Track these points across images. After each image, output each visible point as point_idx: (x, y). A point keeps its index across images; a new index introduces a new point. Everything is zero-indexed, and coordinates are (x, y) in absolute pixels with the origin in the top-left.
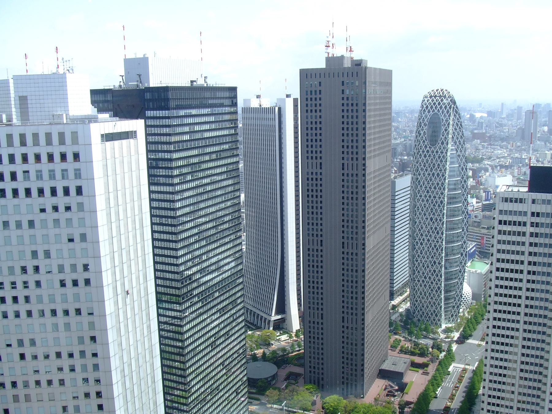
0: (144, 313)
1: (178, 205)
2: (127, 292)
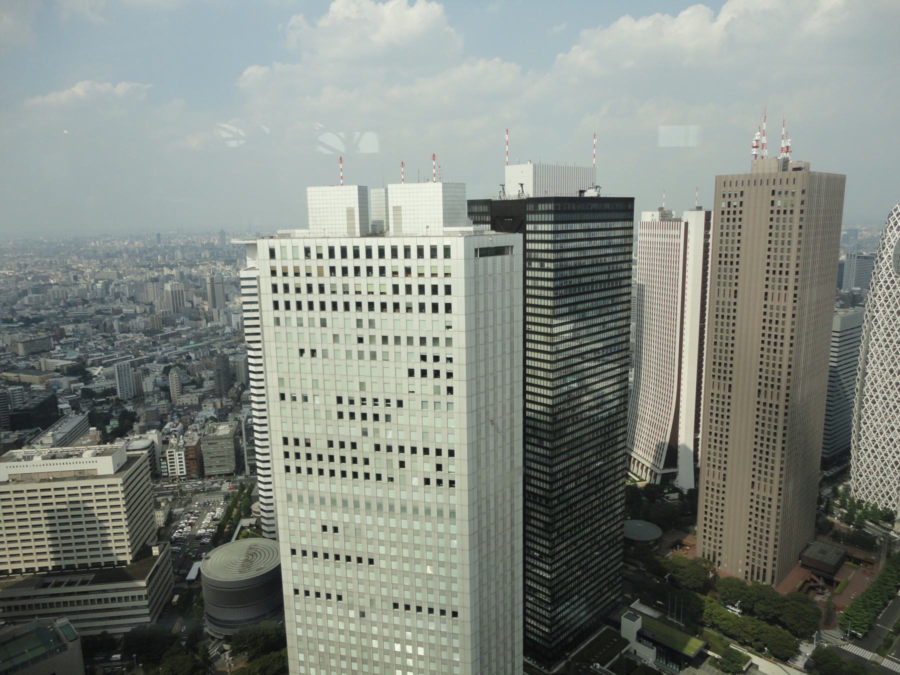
1: (556, 330)
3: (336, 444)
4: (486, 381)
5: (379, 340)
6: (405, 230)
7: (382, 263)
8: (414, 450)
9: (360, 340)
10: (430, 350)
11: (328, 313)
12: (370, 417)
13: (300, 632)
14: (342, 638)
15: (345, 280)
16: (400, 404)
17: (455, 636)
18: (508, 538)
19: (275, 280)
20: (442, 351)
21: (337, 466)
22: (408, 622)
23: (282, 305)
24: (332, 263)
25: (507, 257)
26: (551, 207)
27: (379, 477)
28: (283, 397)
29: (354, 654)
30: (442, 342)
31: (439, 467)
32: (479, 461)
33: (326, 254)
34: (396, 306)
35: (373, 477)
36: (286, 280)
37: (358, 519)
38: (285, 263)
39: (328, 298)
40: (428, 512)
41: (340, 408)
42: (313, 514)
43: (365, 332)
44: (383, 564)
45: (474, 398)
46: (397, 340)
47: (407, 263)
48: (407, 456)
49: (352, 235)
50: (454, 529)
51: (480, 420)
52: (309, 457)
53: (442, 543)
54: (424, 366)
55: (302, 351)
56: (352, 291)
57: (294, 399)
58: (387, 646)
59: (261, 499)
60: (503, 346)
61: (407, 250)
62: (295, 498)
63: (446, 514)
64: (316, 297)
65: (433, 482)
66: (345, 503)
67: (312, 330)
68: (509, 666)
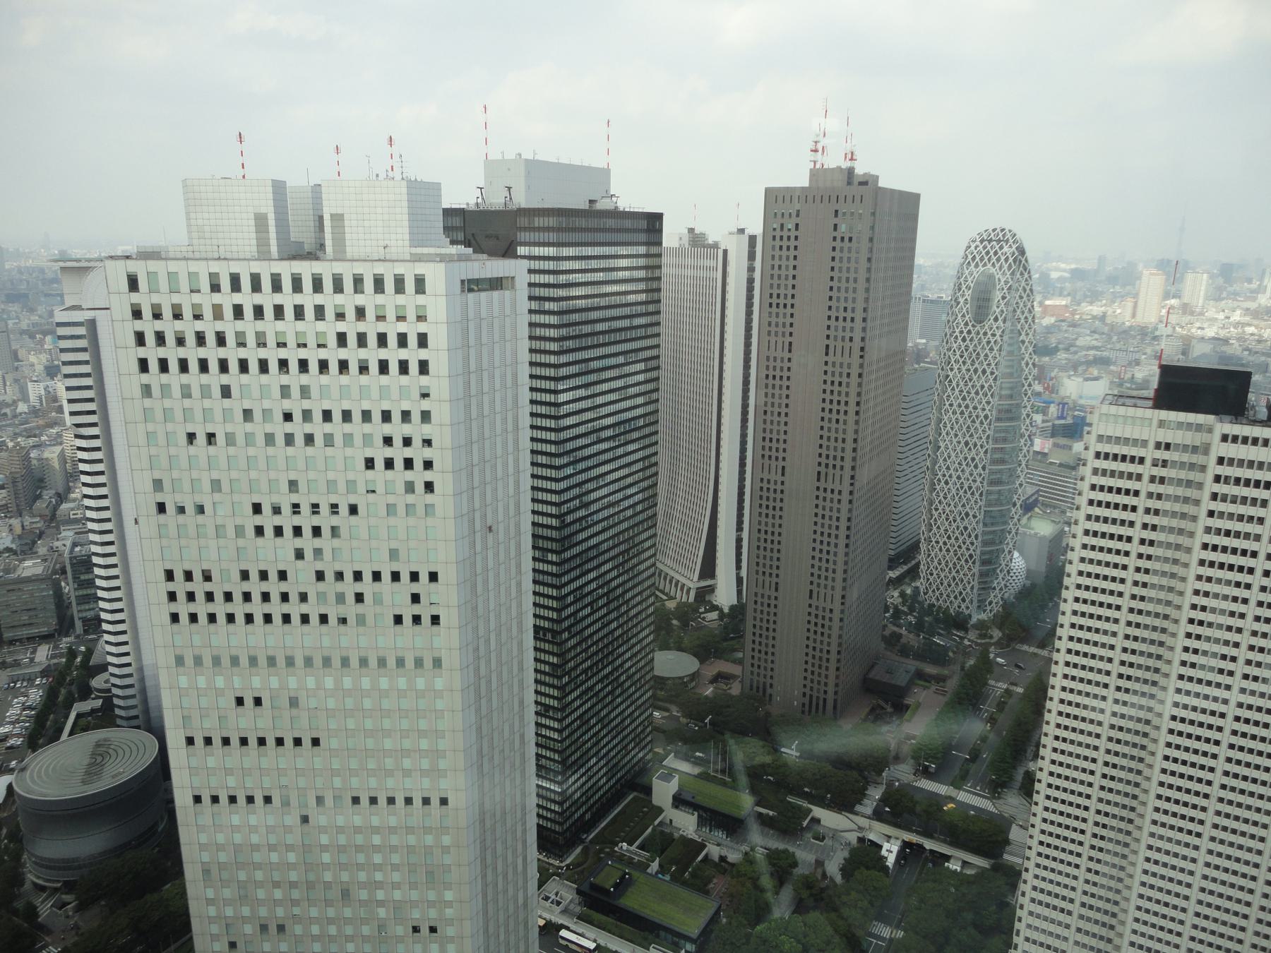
0: (513, 562)
2: (490, 528)
3: (254, 575)
4: (483, 471)
5: (317, 416)
6: (350, 251)
7: (319, 299)
8: (377, 576)
9: (288, 417)
10: (397, 429)
11: (233, 377)
12: (307, 532)
13: (206, 857)
14: (274, 857)
15: (260, 326)
16: (353, 510)
17: (444, 830)
18: (516, 690)
19: (139, 325)
20: (416, 430)
21: (257, 608)
22: (375, 821)
23: (153, 366)
24: (237, 298)
25: (507, 293)
26: (551, 222)
27: (324, 619)
28: (161, 508)
29: (293, 876)
30: (416, 417)
31: (416, 598)
32: (474, 586)
33: (225, 284)
34: (343, 365)
35: (315, 619)
36: (159, 326)
37: (293, 683)
38: (156, 299)
39: (232, 354)
40: (400, 662)
41: (258, 520)
42: (220, 682)
43: (295, 405)
44: (334, 743)
45: (465, 496)
46: (347, 416)
47: (360, 300)
48: (367, 586)
49: (263, 255)
50: (439, 683)
51: (479, 529)
52: (210, 597)
53: (422, 704)
54: (388, 452)
55: (191, 437)
56: (271, 342)
57: (181, 510)
58: (344, 859)
59: (111, 669)
60: (505, 420)
61: (358, 281)
62: (189, 661)
63: (428, 663)
64: (212, 353)
65: (407, 620)
66: (272, 661)
67: (207, 403)
68: (520, 861)
